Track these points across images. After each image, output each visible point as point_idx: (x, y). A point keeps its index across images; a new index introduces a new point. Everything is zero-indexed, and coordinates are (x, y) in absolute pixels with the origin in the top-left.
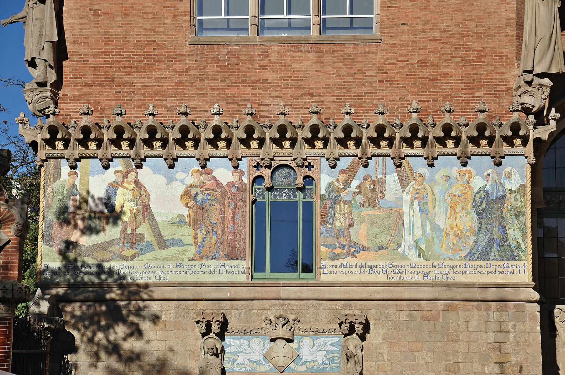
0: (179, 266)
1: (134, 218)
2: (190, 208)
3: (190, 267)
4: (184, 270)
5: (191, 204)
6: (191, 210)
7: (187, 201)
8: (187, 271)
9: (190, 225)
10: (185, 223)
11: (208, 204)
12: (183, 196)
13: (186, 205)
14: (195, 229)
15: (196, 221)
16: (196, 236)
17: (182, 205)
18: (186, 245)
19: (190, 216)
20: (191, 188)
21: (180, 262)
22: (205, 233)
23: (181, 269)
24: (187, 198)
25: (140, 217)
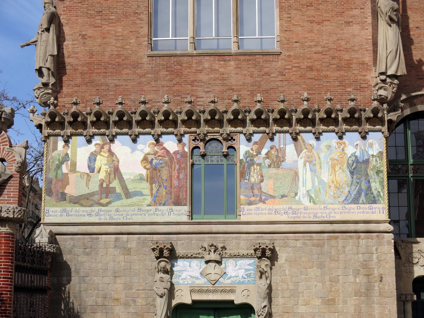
0: (140, 211)
1: (108, 177)
2: (148, 169)
3: (148, 211)
4: (143, 213)
5: (148, 166)
6: (149, 171)
7: (145, 164)
8: (146, 214)
9: (147, 182)
10: (144, 180)
11: (160, 167)
12: (142, 161)
13: (145, 167)
14: (151, 184)
15: (152, 178)
16: (152, 189)
17: (141, 167)
18: (145, 195)
19: (148, 175)
20: (148, 156)
21: (140, 207)
22: (158, 187)
23: (141, 212)
24: (145, 163)
25: (112, 176)
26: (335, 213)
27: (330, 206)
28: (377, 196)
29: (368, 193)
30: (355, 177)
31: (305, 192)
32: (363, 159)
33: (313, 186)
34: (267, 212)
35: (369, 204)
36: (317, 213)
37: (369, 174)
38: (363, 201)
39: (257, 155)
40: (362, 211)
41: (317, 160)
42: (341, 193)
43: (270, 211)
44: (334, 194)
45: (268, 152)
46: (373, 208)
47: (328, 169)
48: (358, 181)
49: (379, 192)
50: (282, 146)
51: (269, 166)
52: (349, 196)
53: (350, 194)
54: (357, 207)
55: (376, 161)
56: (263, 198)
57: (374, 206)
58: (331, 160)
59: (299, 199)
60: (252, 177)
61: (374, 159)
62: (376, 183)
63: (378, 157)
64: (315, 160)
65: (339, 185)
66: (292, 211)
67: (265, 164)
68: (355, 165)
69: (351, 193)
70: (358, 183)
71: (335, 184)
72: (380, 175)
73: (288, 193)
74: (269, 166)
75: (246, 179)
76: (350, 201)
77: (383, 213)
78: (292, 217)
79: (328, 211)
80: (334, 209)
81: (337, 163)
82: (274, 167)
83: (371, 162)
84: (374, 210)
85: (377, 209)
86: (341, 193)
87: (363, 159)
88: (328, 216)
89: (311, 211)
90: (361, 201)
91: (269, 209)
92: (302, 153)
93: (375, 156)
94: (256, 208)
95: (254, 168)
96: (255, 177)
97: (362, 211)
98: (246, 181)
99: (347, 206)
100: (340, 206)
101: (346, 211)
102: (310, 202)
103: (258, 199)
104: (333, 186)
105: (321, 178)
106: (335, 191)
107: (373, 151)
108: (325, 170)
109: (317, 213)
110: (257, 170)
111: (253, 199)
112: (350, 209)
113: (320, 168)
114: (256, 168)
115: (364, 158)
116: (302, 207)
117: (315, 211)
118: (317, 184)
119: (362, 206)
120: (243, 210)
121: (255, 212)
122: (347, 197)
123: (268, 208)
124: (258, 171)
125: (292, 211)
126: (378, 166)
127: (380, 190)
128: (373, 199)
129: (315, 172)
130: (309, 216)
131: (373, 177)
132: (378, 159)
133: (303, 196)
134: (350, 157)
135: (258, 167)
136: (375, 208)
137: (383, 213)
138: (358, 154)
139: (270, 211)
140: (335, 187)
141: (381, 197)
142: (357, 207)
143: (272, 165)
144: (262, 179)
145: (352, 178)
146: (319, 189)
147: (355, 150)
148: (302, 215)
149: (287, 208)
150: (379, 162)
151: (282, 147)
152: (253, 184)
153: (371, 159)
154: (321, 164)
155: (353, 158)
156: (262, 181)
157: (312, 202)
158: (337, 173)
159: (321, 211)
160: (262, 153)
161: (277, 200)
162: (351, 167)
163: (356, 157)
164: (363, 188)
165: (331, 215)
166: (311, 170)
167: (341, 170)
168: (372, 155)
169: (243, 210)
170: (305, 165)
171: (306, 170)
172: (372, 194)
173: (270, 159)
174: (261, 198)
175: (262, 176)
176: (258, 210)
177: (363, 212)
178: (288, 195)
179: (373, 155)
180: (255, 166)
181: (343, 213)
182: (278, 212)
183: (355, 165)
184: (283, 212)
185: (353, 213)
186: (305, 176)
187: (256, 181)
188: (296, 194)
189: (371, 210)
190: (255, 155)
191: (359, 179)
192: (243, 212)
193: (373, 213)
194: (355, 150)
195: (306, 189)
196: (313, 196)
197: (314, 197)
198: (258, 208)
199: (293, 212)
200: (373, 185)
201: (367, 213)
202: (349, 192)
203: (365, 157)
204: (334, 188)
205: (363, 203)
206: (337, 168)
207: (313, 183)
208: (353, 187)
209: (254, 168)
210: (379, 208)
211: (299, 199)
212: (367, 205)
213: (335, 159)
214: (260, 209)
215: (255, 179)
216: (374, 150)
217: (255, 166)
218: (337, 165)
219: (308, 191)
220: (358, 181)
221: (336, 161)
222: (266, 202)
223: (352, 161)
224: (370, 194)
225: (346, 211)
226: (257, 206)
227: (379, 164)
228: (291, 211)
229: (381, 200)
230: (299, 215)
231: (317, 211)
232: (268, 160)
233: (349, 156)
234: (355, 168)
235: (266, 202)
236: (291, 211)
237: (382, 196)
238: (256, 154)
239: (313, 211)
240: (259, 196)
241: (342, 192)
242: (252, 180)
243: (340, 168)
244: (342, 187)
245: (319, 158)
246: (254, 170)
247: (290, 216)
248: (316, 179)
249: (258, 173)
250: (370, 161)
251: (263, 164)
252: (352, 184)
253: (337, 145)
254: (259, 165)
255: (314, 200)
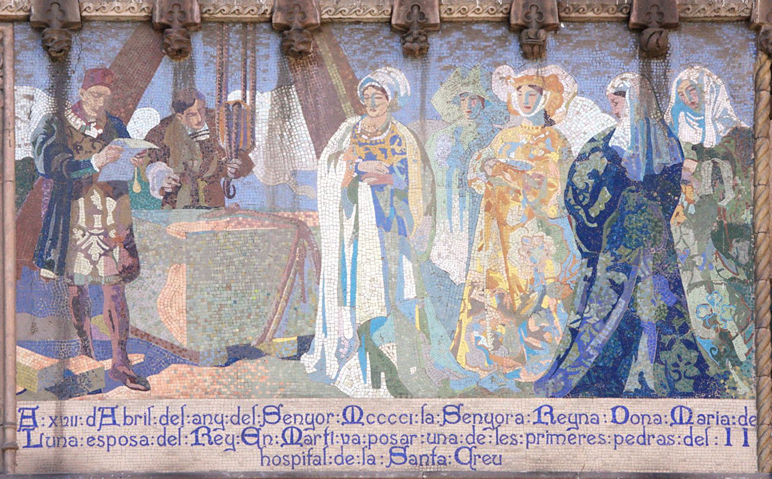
26: (499, 441)
27: (470, 405)
28: (718, 357)
29: (672, 342)
30: (604, 259)
31: (349, 334)
32: (649, 164)
33: (391, 305)
34: (154, 432)
35: (673, 394)
36: (408, 441)
37: (680, 247)
38: (642, 381)
39: (104, 140)
40: (637, 430)
41: (414, 169)
42: (530, 340)
43: (172, 430)
44: (497, 344)
45: (165, 122)
46: (695, 419)
47: (466, 214)
48: (621, 277)
49: (725, 336)
50: (234, 95)
51: (169, 199)
52: (574, 355)
53: (575, 346)
54: (614, 410)
55: (717, 176)
56: (136, 359)
57: (700, 405)
58: (482, 169)
59: (321, 365)
60: (81, 256)
61: (708, 166)
62: (710, 291)
63: (727, 157)
64: (404, 171)
65: (525, 299)
66: (282, 426)
67: (145, 184)
68: (605, 195)
69: (585, 338)
70: (618, 289)
71: (501, 296)
72: (733, 252)
73: (264, 336)
74: (169, 199)
75: (50, 266)
76: (575, 380)
77: (746, 444)
78: (281, 460)
79: (462, 429)
80: (494, 421)
81: (514, 185)
82: (195, 204)
83: (686, 183)
84: (698, 431)
85: (713, 421)
86: (530, 340)
87: (649, 164)
88: (464, 455)
89: (378, 429)
90: (632, 384)
91: (169, 419)
92: (338, 135)
93: (711, 153)
94: (99, 414)
95: (89, 203)
96: (95, 251)
97: (637, 430)
98: (45, 273)
99: (564, 406)
100: (527, 405)
101: (558, 429)
102: (376, 384)
103: (108, 364)
104: (493, 301)
105: (429, 260)
106: (502, 330)
107: (702, 124)
108: (455, 219)
109: (408, 441)
110: (104, 220)
111: (82, 365)
112: (576, 420)
113: (431, 210)
114: (100, 207)
115: (656, 161)
116: (336, 406)
117: (399, 430)
118: (410, 291)
119: (637, 406)
120: (29, 422)
121: (93, 431)
122: (560, 360)
123: (158, 412)
124: (110, 220)
125: (282, 426)
126: (723, 203)
127: (731, 327)
128: (695, 371)
129: (403, 232)
130: (368, 452)
131: (699, 261)
132: (726, 169)
133: (338, 354)
134: (582, 157)
135: (111, 204)
136: (704, 419)
137: (746, 444)
138: (622, 140)
139: (172, 430)
140: (501, 307)
141: (736, 362)
142: (614, 410)
143: (184, 196)
144: (129, 261)
145: (592, 262)
146: (423, 316)
147: (611, 122)
148: (332, 451)
149: (259, 411)
150: (728, 185)
151: (237, 103)
152: (80, 288)
153: (690, 165)
154: (433, 191)
155: (599, 163)
156: (130, 272)
157: (384, 384)
158: (514, 237)
159: (428, 428)
160: (130, 127)
161: (205, 374)
162: (586, 208)
163: (614, 156)
164: (644, 318)
165: (481, 451)
166: (383, 222)
167: (532, 224)
168: (694, 148)
169: (29, 422)
170: (351, 193)
171: (356, 227)
172: (691, 345)
173: (171, 160)
174: (126, 362)
175: (131, 249)
176: (110, 420)
177: (645, 439)
178: (263, 347)
179: (698, 149)
180: (96, 198)
181: (543, 440)
182: (213, 434)
183: (605, 195)
184: (238, 429)
185: (590, 439)
186: (349, 252)
187: (101, 272)
188: (305, 344)
189: (684, 430)
190: (93, 140)
191: (627, 270)
192: (28, 430)
193: (692, 441)
194: (609, 121)
195: (353, 319)
196: (390, 351)
197: (394, 360)
198: (108, 412)
199: (288, 433)
200: (695, 298)
201: (664, 441)
202: (574, 333)
203: (659, 156)
204: (497, 316)
205: (644, 393)
206: (514, 211)
207: (392, 282)
208: (593, 313)
209: (89, 203)
210: (725, 421)
211: (321, 365)
212: (662, 406)
213: (506, 167)
214: (119, 419)
215: (94, 263)
216: (708, 120)
217: (96, 198)
218: (516, 199)
219: (365, 331)
220: (621, 277)
221: (508, 176)
222: (153, 380)
223: (594, 174)
224: (678, 347)
225: (558, 429)
226: (99, 404)
227: (730, 195)
228: (275, 430)
229: (737, 379)
230: (318, 449)
231: (409, 430)
232: (160, 166)
233: (576, 150)
234: (601, 218)
235: (153, 380)
236: (275, 430)
237: (743, 358)
238: (100, 136)
239: (386, 429)
240: (115, 347)
241: (539, 335)
242: (81, 268)
243: (531, 216)
244: (538, 309)
245: (425, 160)
246: (90, 220)
247: (270, 451)
248: (408, 266)
249: (112, 234)
250: (685, 175)
251: (137, 188)
252: (588, 292)
253: (515, 94)
254: (117, 190)
255: (390, 368)
